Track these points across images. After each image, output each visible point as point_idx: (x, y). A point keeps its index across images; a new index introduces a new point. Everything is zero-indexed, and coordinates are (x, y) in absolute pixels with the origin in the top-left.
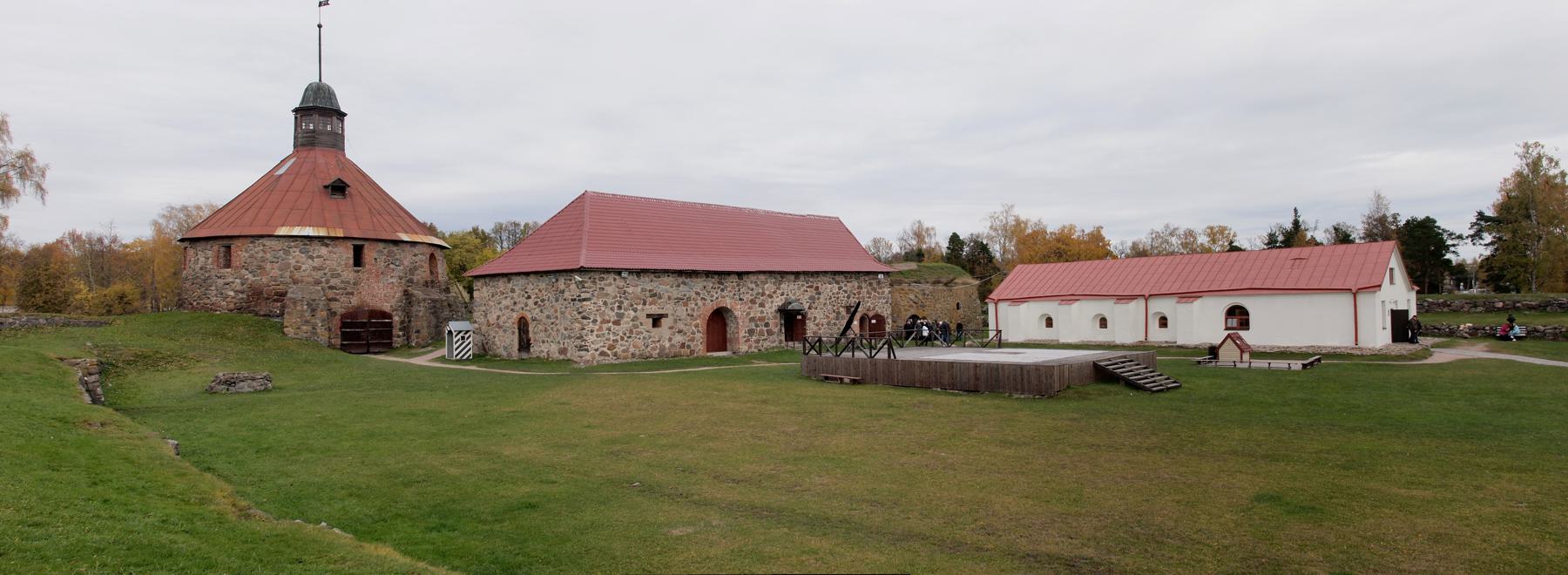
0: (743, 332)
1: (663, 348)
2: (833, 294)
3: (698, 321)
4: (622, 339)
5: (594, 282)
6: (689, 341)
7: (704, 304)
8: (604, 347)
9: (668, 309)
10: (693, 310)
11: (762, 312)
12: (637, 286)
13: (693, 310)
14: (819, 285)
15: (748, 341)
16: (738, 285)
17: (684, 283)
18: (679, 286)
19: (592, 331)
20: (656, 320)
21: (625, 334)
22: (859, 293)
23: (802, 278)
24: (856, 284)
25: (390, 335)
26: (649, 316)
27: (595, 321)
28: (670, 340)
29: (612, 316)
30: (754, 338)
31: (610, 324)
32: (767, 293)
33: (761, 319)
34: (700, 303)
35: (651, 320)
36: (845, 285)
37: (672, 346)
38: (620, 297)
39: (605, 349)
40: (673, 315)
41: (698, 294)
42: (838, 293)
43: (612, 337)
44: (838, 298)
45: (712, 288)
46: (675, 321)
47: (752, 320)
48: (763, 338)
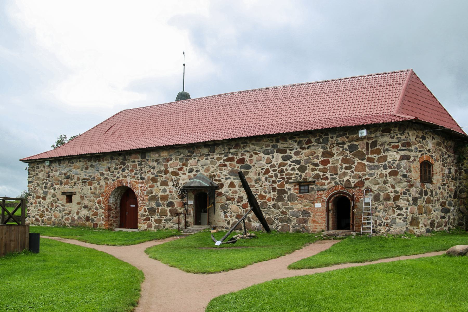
0: (143, 210)
1: (73, 220)
2: (271, 167)
3: (101, 198)
4: (47, 210)
5: (34, 170)
6: (93, 215)
7: (106, 184)
8: (38, 215)
9: (77, 188)
10: (96, 189)
11: (164, 191)
12: (56, 171)
13: (96, 189)
14: (247, 157)
15: (148, 219)
16: (140, 165)
17: (92, 166)
18: (87, 168)
19: (31, 204)
20: (69, 197)
21: (48, 207)
22: (325, 163)
23: (218, 150)
24: (320, 151)
25: (350, 226)
26: (63, 193)
27: (34, 196)
28: (78, 213)
29: (41, 193)
30: (155, 217)
31: (41, 199)
32: (170, 170)
33: (164, 198)
34: (102, 182)
35: (65, 197)
36: (297, 154)
37: (79, 218)
38: (46, 180)
39: (38, 217)
40: (80, 193)
41: (102, 174)
42: (281, 165)
43: (42, 209)
44: (282, 171)
45: (115, 169)
46: (82, 198)
47: (153, 198)
48: (165, 218)
